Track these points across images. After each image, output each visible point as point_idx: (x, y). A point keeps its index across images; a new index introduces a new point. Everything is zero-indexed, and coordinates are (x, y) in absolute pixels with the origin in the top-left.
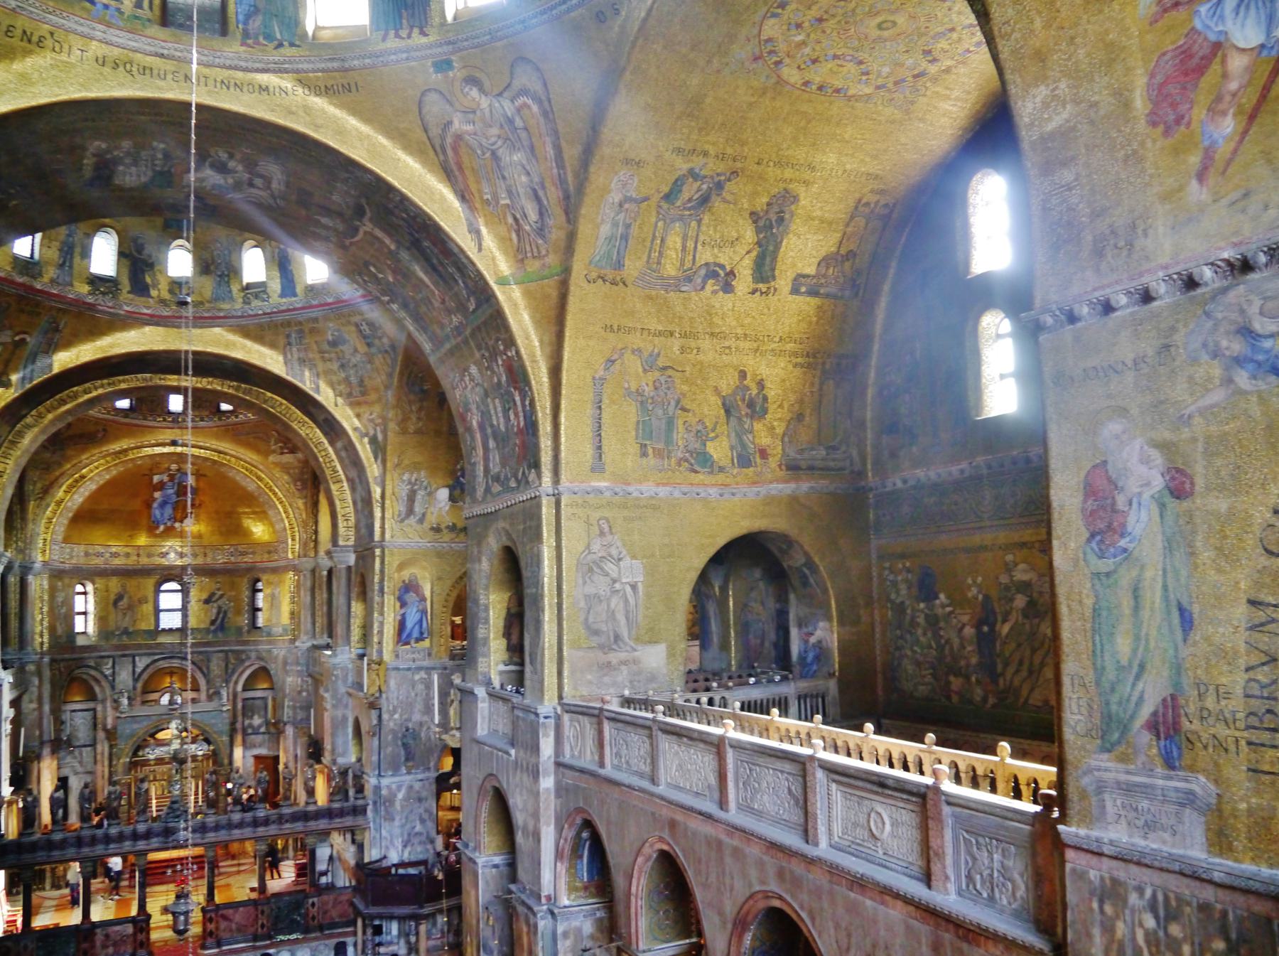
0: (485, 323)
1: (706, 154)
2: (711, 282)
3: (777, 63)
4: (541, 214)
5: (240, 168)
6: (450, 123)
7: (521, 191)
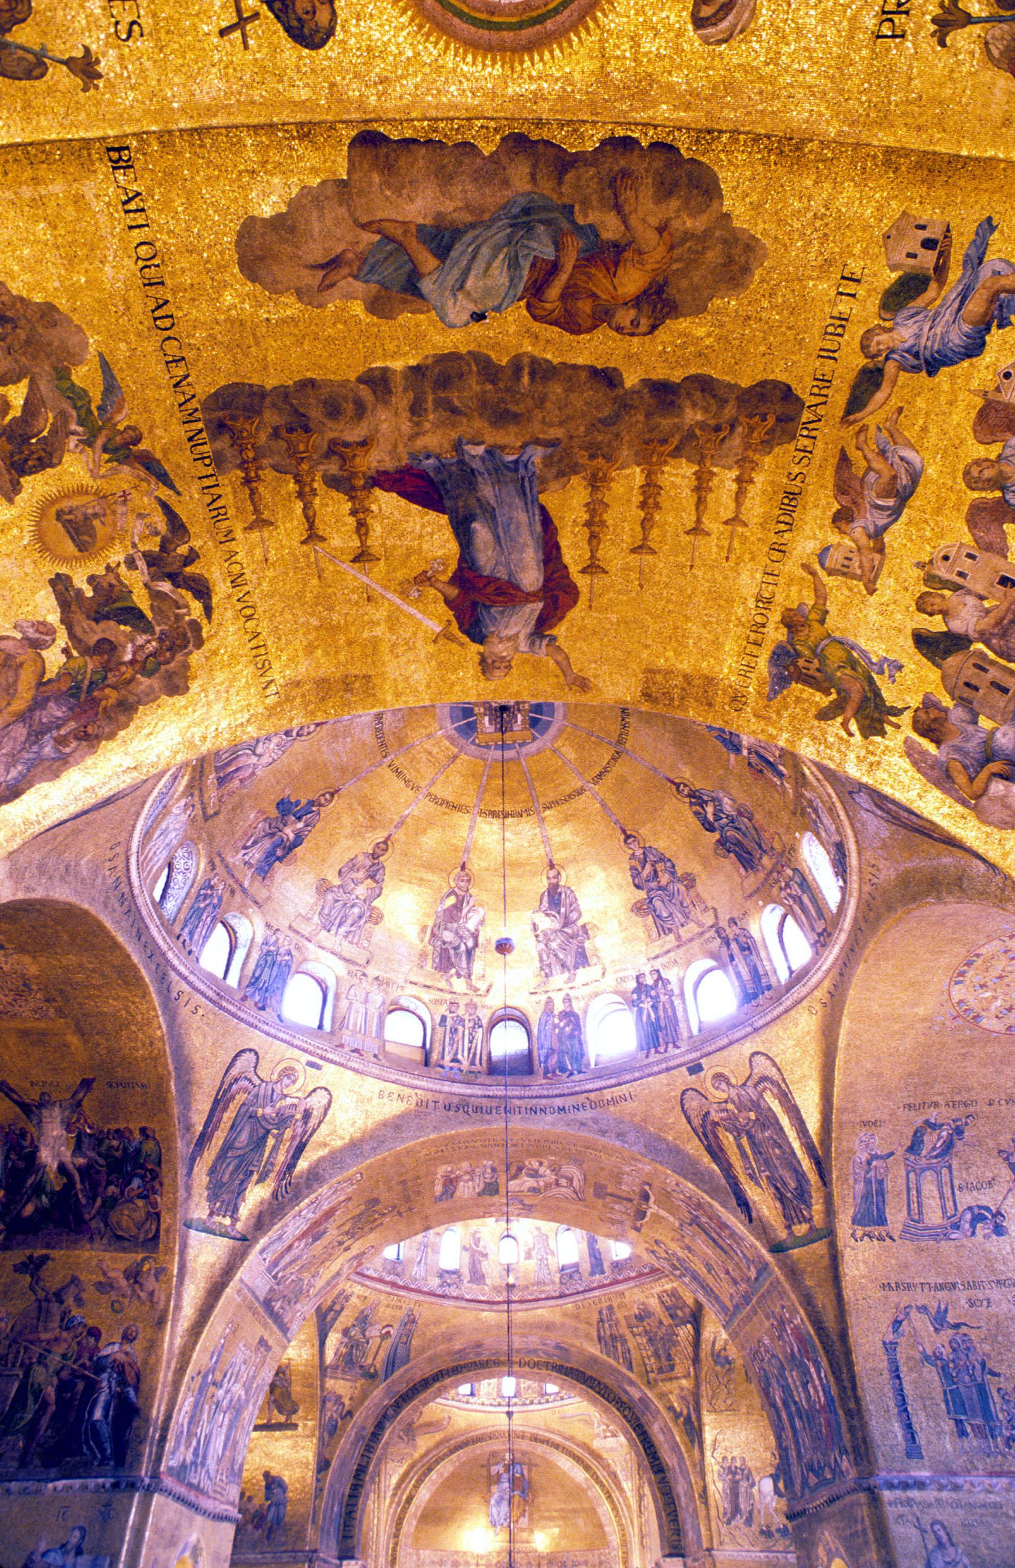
0: (768, 1292)
1: (936, 1105)
2: (979, 1226)
3: (974, 1018)
4: (798, 1181)
5: (548, 1172)
6: (708, 1113)
7: (777, 1162)
